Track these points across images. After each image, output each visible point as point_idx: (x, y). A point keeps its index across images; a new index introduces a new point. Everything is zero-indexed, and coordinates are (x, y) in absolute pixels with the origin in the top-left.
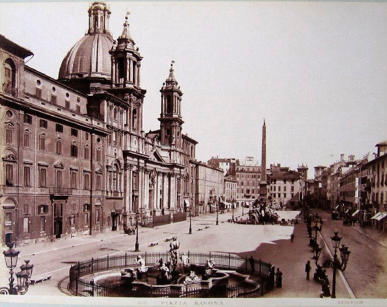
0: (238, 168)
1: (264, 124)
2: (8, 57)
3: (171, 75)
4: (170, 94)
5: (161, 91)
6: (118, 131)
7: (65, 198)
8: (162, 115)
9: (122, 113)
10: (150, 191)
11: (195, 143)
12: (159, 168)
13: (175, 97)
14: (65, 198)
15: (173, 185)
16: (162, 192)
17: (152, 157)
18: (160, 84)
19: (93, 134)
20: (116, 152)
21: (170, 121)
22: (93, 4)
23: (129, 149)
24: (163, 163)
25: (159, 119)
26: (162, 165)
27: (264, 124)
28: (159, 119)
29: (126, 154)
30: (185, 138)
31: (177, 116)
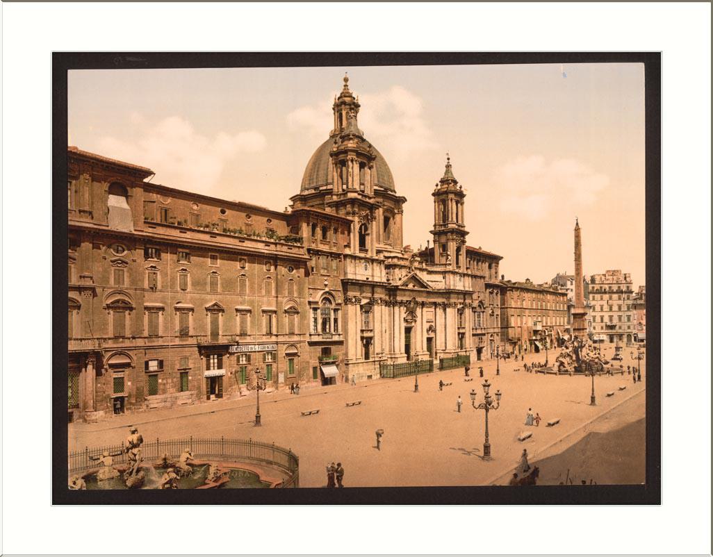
0: (593, 288)
1: (577, 224)
4: (448, 194)
5: (433, 195)
8: (435, 226)
10: (408, 330)
13: (451, 200)
15: (485, 317)
18: (432, 183)
21: (448, 231)
22: (339, 98)
24: (430, 290)
25: (431, 232)
27: (577, 224)
28: (431, 232)
30: (476, 256)
31: (455, 226)
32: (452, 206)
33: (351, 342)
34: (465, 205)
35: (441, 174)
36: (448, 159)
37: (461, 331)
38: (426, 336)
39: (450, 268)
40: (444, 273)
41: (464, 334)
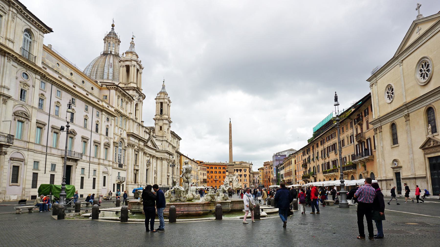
2: (28, 27)
3: (164, 87)
6: (122, 115)
7: (76, 161)
9: (127, 103)
10: (147, 170)
11: (179, 139)
12: (153, 153)
14: (76, 161)
16: (156, 173)
17: (149, 144)
19: (104, 113)
20: (122, 132)
23: (132, 131)
25: (154, 119)
26: (156, 151)
28: (154, 119)
29: (130, 135)
31: (167, 117)
32: (165, 106)
33: (130, 171)
34: (171, 107)
35: (160, 89)
36: (164, 82)
37: (168, 175)
38: (154, 176)
39: (164, 139)
40: (162, 141)
41: (169, 176)
